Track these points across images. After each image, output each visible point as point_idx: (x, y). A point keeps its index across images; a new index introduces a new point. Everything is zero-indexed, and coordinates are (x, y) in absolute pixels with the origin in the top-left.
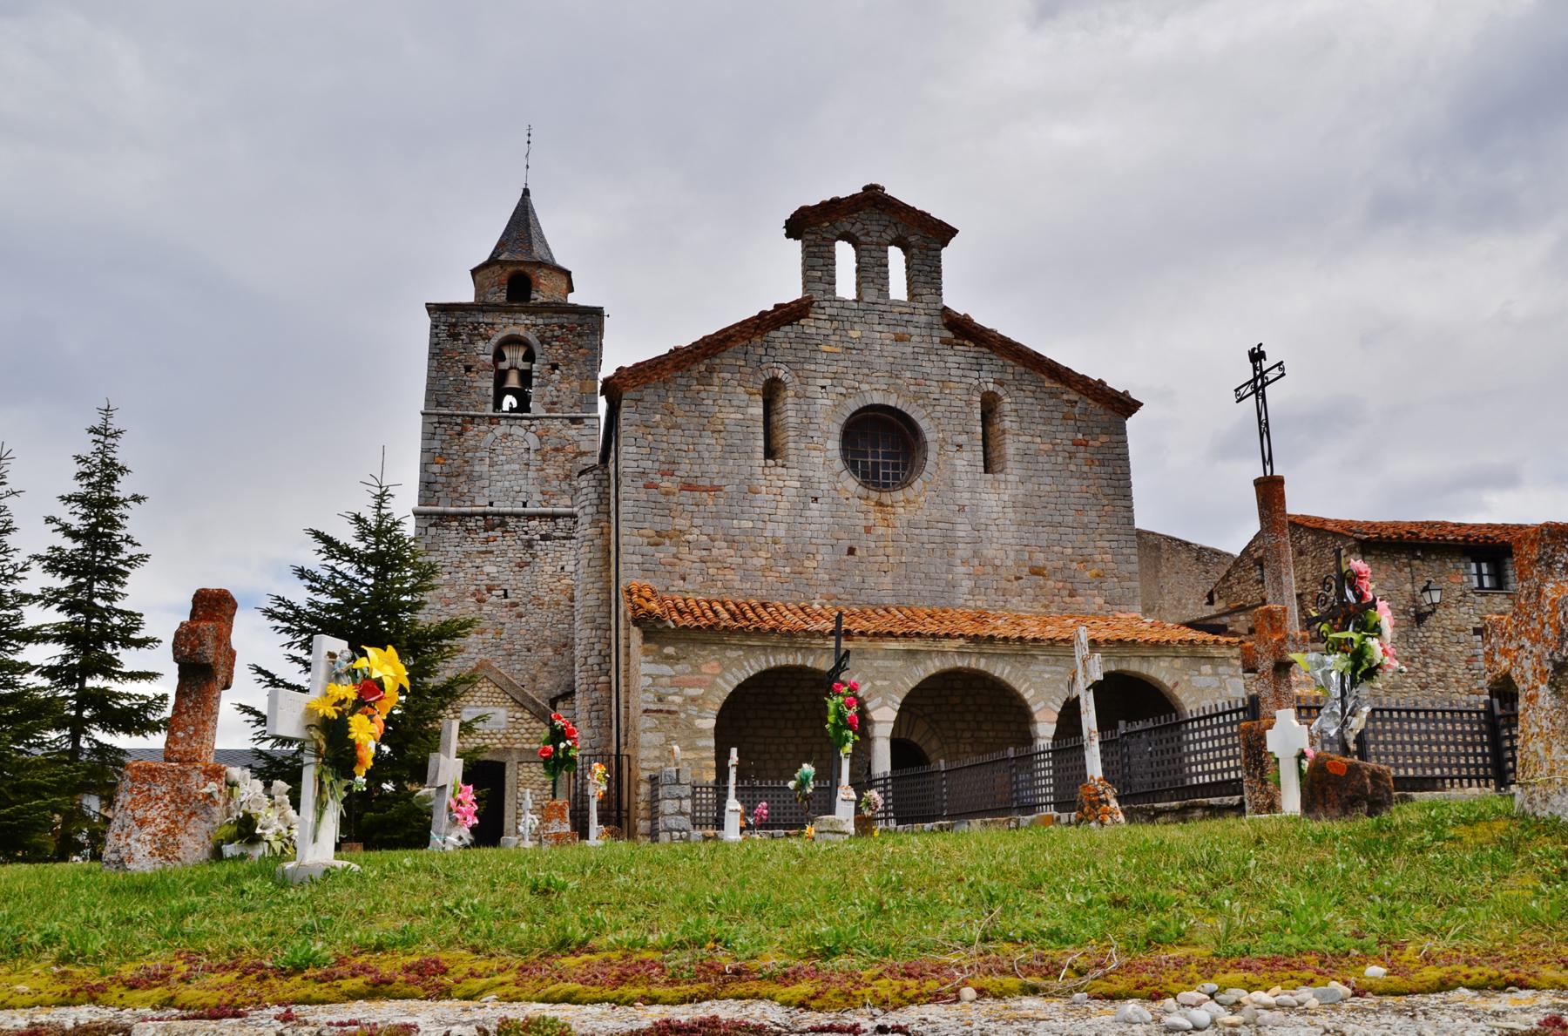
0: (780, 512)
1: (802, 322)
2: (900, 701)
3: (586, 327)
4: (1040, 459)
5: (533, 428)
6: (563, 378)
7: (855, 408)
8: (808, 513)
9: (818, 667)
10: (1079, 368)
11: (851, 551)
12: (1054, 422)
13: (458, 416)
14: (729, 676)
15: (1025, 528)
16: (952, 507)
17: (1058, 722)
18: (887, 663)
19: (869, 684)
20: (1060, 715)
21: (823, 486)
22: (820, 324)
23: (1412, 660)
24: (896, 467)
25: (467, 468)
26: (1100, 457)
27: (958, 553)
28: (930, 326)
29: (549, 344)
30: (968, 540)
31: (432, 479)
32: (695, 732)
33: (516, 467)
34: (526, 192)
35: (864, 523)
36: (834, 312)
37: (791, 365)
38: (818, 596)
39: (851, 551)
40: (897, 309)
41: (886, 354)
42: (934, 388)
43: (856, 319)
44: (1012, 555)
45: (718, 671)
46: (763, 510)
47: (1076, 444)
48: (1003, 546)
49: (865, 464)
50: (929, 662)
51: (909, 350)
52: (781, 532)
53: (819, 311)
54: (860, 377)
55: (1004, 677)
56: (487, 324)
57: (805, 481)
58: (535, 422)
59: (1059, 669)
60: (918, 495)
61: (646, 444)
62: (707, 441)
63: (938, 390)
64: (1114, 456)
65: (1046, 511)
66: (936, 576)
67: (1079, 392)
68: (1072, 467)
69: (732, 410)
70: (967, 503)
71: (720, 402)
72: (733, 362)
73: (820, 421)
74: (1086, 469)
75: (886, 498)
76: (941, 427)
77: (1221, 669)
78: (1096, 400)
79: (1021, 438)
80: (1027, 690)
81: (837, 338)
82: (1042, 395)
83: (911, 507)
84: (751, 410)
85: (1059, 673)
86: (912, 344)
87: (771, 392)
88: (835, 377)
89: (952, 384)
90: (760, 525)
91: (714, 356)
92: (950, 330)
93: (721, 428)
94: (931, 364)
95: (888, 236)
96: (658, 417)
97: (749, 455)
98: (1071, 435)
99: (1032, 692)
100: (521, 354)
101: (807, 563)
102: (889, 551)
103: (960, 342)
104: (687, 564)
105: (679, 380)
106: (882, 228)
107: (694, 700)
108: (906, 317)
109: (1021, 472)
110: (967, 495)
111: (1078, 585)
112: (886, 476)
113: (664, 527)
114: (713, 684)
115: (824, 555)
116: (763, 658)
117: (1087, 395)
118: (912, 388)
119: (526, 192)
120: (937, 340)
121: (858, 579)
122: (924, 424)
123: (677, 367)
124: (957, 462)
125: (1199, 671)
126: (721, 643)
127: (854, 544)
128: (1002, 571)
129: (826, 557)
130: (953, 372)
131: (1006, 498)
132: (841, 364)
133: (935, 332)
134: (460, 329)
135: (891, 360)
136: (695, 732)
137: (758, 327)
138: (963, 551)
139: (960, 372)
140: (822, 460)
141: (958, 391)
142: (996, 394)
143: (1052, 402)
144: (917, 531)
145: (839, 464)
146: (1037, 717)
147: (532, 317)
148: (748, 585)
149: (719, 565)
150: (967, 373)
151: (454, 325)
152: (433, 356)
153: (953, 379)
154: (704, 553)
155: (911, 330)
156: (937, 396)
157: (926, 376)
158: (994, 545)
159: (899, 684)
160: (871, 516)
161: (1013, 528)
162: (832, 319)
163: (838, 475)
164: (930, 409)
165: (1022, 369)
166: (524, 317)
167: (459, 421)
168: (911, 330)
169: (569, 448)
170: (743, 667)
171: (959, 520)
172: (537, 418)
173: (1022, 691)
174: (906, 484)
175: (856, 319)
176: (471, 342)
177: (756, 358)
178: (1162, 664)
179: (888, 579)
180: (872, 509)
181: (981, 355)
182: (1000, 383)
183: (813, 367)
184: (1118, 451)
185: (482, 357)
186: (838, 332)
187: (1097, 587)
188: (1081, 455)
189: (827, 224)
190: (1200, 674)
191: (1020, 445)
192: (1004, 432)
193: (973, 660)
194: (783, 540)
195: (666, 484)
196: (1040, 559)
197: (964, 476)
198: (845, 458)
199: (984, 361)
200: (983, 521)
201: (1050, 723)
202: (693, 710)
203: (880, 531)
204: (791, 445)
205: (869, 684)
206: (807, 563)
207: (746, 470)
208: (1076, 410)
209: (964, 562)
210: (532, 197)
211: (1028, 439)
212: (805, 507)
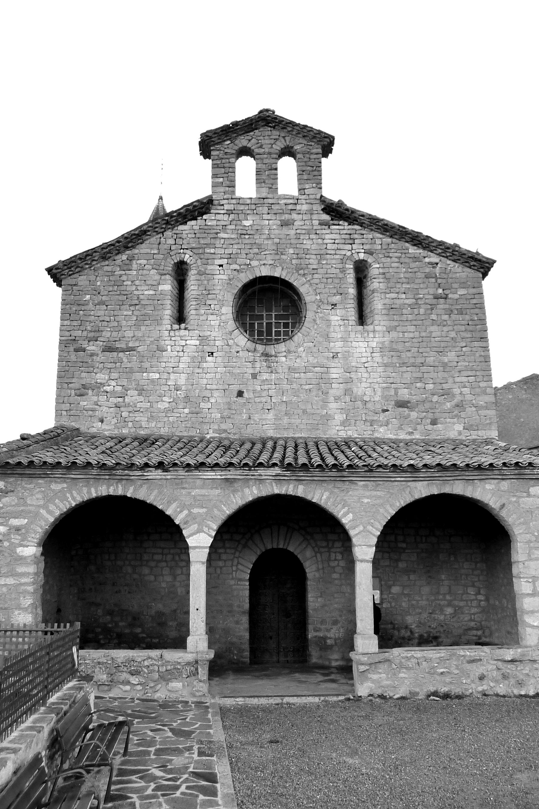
0: (181, 365)
1: (205, 217)
2: (215, 527)
4: (405, 311)
8: (205, 365)
9: (138, 497)
10: (438, 236)
11: (240, 394)
12: (417, 281)
14: (52, 507)
15: (390, 369)
17: (377, 546)
18: (204, 492)
19: (186, 512)
20: (379, 537)
21: (217, 343)
22: (219, 217)
24: (286, 325)
26: (458, 307)
27: (331, 392)
28: (311, 212)
30: (341, 380)
32: (16, 560)
35: (251, 371)
36: (231, 207)
37: (194, 251)
38: (211, 431)
39: (240, 394)
40: (283, 202)
41: (272, 236)
42: (313, 261)
43: (248, 212)
44: (379, 393)
45: (41, 502)
46: (168, 364)
47: (437, 297)
49: (260, 325)
50: (247, 491)
51: (292, 232)
52: (182, 380)
53: (219, 207)
54: (249, 256)
55: (322, 503)
59: (379, 493)
60: (299, 346)
61: (77, 318)
62: (125, 313)
63: (316, 262)
64: (473, 306)
65: (409, 354)
66: (312, 411)
67: (439, 255)
68: (434, 317)
69: (146, 288)
70: (339, 350)
71: (137, 283)
72: (148, 251)
73: (217, 292)
74: (446, 317)
75: (271, 349)
76: (318, 291)
78: (454, 261)
79: (388, 296)
80: (345, 515)
81: (233, 227)
82: (407, 260)
83: (292, 356)
84: (161, 287)
85: (380, 497)
86: (295, 228)
88: (230, 257)
90: (165, 376)
91: (133, 247)
92: (328, 213)
93: (137, 302)
95: (279, 145)
96: (88, 297)
97: (158, 321)
98: (432, 291)
99: (350, 516)
101: (202, 405)
102: (271, 393)
103: (336, 222)
104: (105, 409)
105: (106, 268)
106: (272, 142)
107: (18, 529)
108: (290, 207)
109: (387, 323)
110: (339, 344)
111: (437, 415)
112: (278, 333)
113: (88, 381)
114: (37, 514)
115: (217, 397)
116: (85, 490)
117: (447, 257)
118: (294, 262)
120: (316, 223)
121: (245, 416)
122: (302, 290)
123: (104, 258)
124: (333, 318)
125: (528, 492)
126: (46, 476)
127: (242, 388)
128: (369, 405)
129: (219, 400)
130: (329, 246)
131: (374, 345)
132: (235, 246)
133: (315, 217)
135: (277, 241)
136: (16, 560)
137: (168, 223)
138: (337, 389)
139: (335, 246)
141: (334, 262)
142: (366, 261)
143: (413, 265)
144: (297, 375)
145: (231, 324)
146: (354, 540)
148: (153, 425)
149: (131, 409)
153: (329, 252)
154: (120, 400)
155: (294, 216)
156: (315, 267)
157: (307, 252)
158: (364, 385)
159: (216, 511)
160: (258, 365)
161: (380, 369)
162: (229, 212)
163: (231, 333)
164: (309, 277)
165: (389, 240)
168: (294, 216)
170: (66, 499)
171: (333, 365)
174: (289, 336)
175: (248, 212)
178: (488, 487)
180: (258, 359)
181: (354, 232)
182: (370, 253)
183: (212, 251)
184: (474, 301)
186: (234, 222)
187: (456, 416)
188: (441, 306)
189: (229, 142)
190: (529, 496)
191: (387, 301)
192: (373, 292)
193: (291, 487)
194: (183, 388)
195: (91, 348)
196: (404, 394)
199: (356, 236)
200: (353, 364)
201: (370, 546)
202: (16, 538)
203: (265, 376)
204: (193, 312)
205: (186, 512)
206: (202, 405)
207: (155, 334)
208: (437, 270)
209: (337, 399)
211: (395, 295)
212: (203, 360)
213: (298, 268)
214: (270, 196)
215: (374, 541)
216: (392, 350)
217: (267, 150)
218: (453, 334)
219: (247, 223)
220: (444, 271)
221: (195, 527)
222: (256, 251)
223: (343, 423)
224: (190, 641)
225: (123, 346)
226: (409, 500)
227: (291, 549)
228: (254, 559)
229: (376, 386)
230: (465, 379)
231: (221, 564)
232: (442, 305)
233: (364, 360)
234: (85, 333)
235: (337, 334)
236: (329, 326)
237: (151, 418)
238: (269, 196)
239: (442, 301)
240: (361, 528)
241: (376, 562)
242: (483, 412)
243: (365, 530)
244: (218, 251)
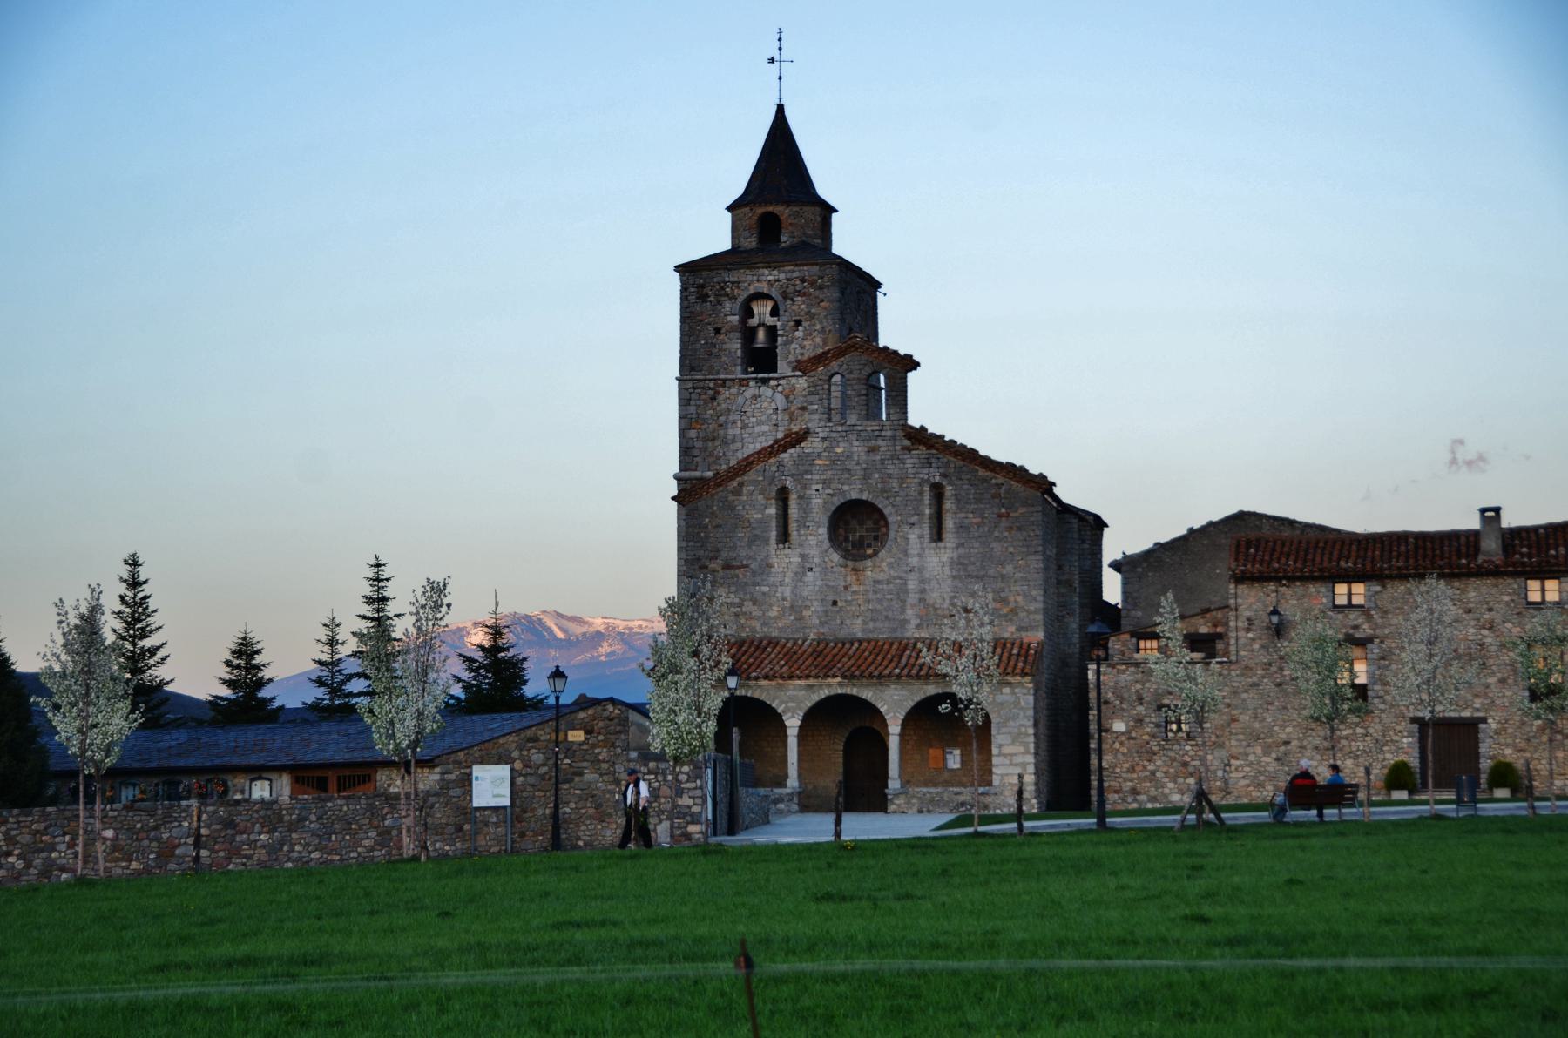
0: (787, 580)
1: (802, 445)
3: (826, 278)
5: (780, 388)
6: (808, 335)
7: (838, 504)
8: (806, 579)
11: (835, 603)
13: (710, 380)
16: (905, 568)
17: (902, 725)
18: (795, 693)
22: (815, 444)
23: (1270, 665)
25: (721, 432)
28: (894, 438)
29: (792, 299)
31: (690, 445)
33: (765, 428)
34: (780, 109)
39: (835, 603)
42: (895, 484)
44: (947, 601)
50: (821, 692)
51: (878, 458)
52: (788, 591)
55: (868, 699)
56: (733, 283)
57: (804, 557)
58: (782, 382)
60: (882, 560)
68: (996, 534)
74: (1006, 534)
75: (860, 565)
77: (1016, 690)
79: (958, 516)
81: (826, 454)
83: (877, 570)
87: (783, 496)
89: (909, 480)
92: (909, 439)
94: (893, 467)
96: (707, 520)
97: (766, 541)
98: (995, 510)
99: (886, 707)
100: (769, 309)
101: (805, 613)
102: (860, 602)
108: (877, 433)
115: (816, 607)
119: (780, 109)
120: (898, 448)
121: (839, 622)
122: (886, 511)
128: (939, 612)
129: (819, 609)
131: (945, 559)
132: (829, 472)
134: (707, 290)
135: (864, 466)
138: (913, 598)
139: (914, 471)
140: (815, 542)
144: (881, 587)
145: (827, 544)
146: (888, 722)
147: (775, 272)
150: (920, 470)
151: (702, 286)
152: (683, 320)
155: (880, 442)
157: (890, 476)
160: (849, 579)
162: (824, 440)
163: (826, 551)
165: (961, 463)
166: (767, 272)
172: (784, 378)
173: (879, 706)
176: (719, 303)
177: (771, 474)
179: (859, 621)
183: (810, 477)
185: (730, 318)
197: (915, 546)
198: (831, 539)
199: (933, 460)
203: (855, 588)
204: (795, 533)
206: (805, 613)
208: (1002, 491)
209: (913, 606)
212: (804, 574)
213: (883, 491)
214: (859, 423)
215: (900, 722)
216: (961, 564)
217: (856, 376)
218: (1011, 550)
219: (839, 450)
220: (1008, 491)
221: (790, 714)
222: (847, 476)
223: (918, 627)
224: (789, 783)
225: (738, 564)
226: (923, 696)
227: (875, 727)
228: (847, 734)
229: (945, 596)
230: (1018, 588)
231: (821, 738)
232: (1004, 523)
233: (936, 573)
234: (707, 553)
235: (914, 549)
236: (908, 544)
237: (764, 624)
238: (859, 423)
239: (1003, 519)
240: (892, 714)
241: (902, 735)
242: (1032, 617)
243: (895, 715)
244: (817, 477)
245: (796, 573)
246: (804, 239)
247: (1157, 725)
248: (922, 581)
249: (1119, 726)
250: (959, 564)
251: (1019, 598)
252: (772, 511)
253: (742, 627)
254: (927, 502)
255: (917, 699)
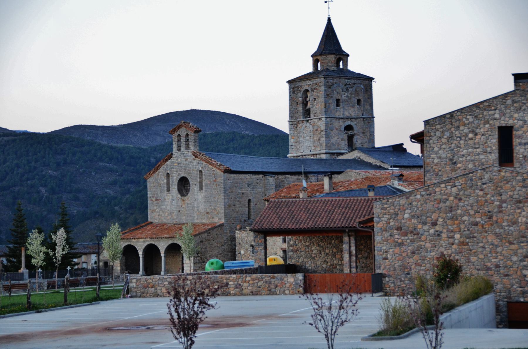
5: (311, 123)
11: (179, 211)
34: (329, 19)
48: (202, 208)
58: (312, 121)
119: (329, 19)
122: (190, 180)
134: (295, 89)
145: (177, 192)
167: (296, 123)
169: (319, 129)
179: (184, 217)
196: (208, 210)
208: (215, 172)
210: (332, 21)
212: (172, 202)
213: (189, 173)
216: (206, 197)
219: (179, 160)
223: (197, 219)
241: (164, 257)
244: (175, 169)
245: (171, 201)
246: (328, 67)
247: (251, 252)
248: (198, 204)
249: (242, 252)
250: (205, 197)
251: (219, 209)
252: (165, 181)
253: (160, 219)
254: (198, 177)
255: (167, 245)
